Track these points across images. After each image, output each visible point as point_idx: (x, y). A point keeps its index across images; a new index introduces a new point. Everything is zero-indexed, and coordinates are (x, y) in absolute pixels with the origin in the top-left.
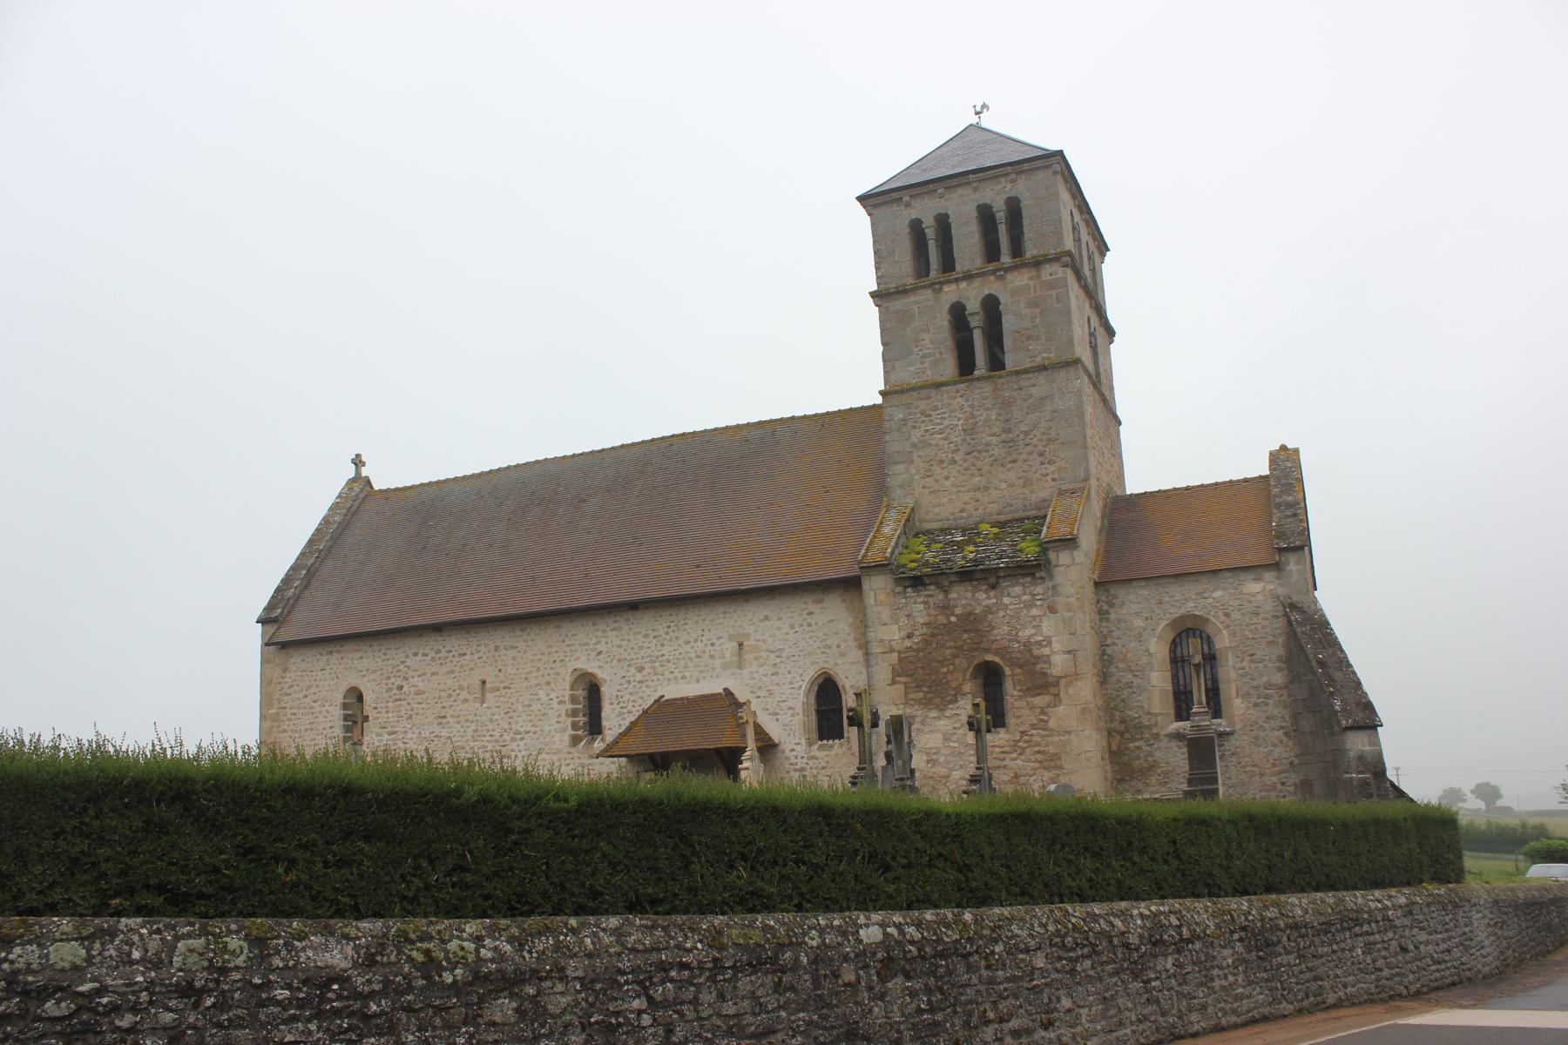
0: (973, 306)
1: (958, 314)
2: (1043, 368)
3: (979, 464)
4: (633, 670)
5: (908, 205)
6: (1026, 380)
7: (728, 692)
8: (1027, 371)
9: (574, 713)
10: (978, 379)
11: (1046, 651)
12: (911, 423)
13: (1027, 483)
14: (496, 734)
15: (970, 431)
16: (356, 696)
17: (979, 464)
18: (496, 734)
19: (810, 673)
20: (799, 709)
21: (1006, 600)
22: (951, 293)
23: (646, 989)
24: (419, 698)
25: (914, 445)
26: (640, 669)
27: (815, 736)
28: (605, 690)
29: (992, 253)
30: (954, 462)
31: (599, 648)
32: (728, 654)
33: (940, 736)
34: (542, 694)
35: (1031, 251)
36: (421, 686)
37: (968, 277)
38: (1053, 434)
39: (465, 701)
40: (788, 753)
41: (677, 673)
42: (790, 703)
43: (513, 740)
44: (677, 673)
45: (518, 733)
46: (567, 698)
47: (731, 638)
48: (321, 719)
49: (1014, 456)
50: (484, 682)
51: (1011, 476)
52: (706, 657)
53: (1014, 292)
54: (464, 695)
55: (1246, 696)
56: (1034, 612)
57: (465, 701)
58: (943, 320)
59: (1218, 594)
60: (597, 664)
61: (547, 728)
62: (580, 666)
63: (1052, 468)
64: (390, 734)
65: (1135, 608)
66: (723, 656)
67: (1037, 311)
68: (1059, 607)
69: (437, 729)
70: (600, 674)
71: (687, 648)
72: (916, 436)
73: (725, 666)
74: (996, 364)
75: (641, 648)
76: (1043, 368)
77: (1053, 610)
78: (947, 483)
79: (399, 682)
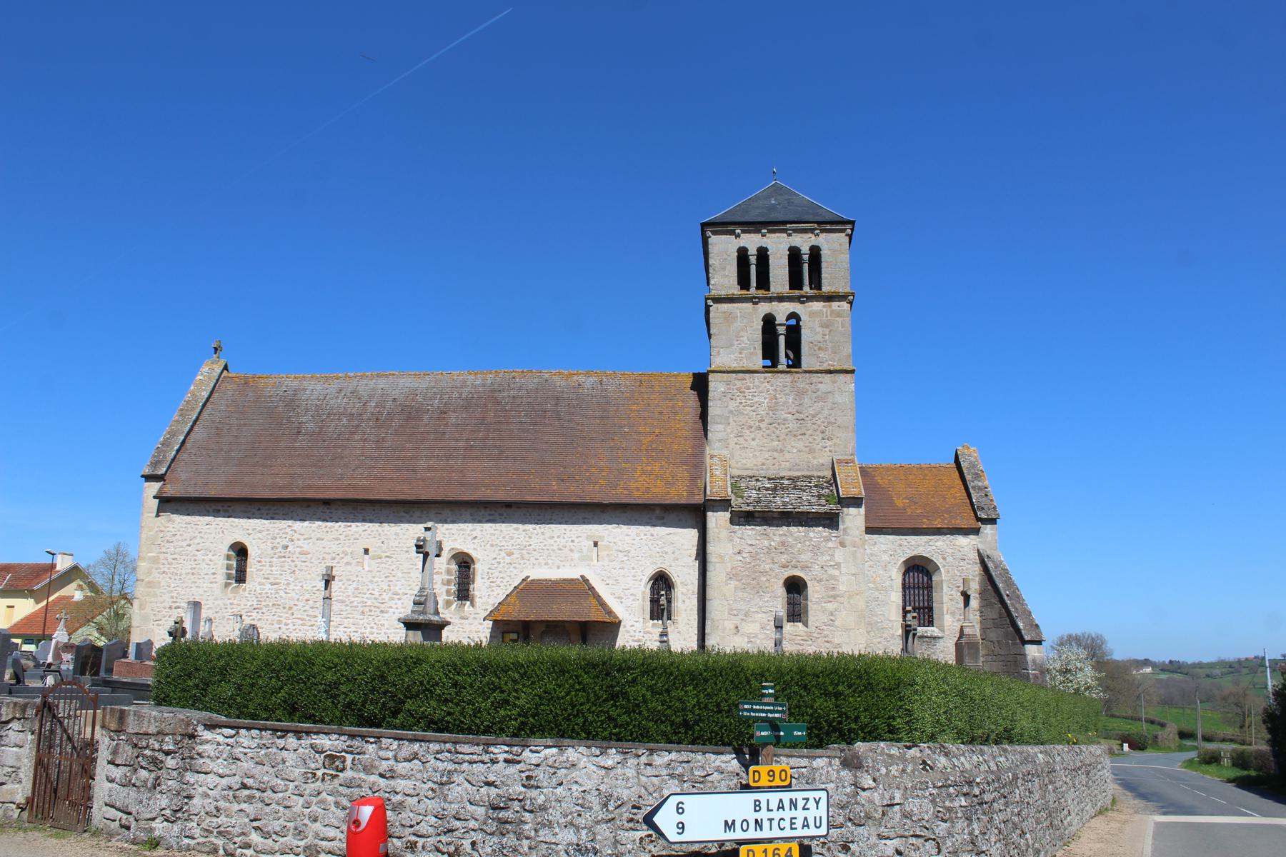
0: (781, 319)
1: (769, 321)
2: (830, 372)
3: (777, 432)
4: (503, 554)
5: (738, 236)
6: (815, 378)
7: (585, 580)
8: (817, 372)
9: (448, 582)
10: (782, 372)
11: (836, 572)
12: (729, 396)
13: (811, 451)
14: (376, 593)
15: (773, 408)
16: (240, 551)
17: (777, 432)
18: (376, 593)
19: (651, 571)
20: (639, 596)
21: (812, 534)
22: (765, 308)
23: (520, 801)
24: (303, 558)
25: (731, 412)
26: (510, 554)
27: (648, 616)
28: (479, 569)
29: (795, 282)
30: (760, 428)
31: (475, 534)
32: (585, 550)
33: (758, 625)
35: (826, 288)
36: (306, 548)
37: (781, 298)
38: (832, 420)
39: (348, 563)
40: (628, 628)
41: (541, 560)
42: (632, 591)
43: (392, 599)
44: (541, 560)
46: (443, 570)
47: (588, 538)
48: (203, 565)
49: (803, 431)
51: (800, 444)
52: (566, 550)
53: (812, 314)
54: (348, 559)
55: (953, 613)
56: (830, 544)
57: (348, 563)
58: (759, 325)
59: (938, 544)
63: (829, 443)
64: (272, 584)
65: (883, 547)
66: (580, 551)
67: (827, 331)
68: (847, 543)
70: (474, 554)
71: (551, 542)
72: (732, 405)
73: (582, 559)
74: (796, 363)
75: (512, 538)
76: (830, 372)
77: (842, 544)
78: (754, 443)
79: (285, 542)
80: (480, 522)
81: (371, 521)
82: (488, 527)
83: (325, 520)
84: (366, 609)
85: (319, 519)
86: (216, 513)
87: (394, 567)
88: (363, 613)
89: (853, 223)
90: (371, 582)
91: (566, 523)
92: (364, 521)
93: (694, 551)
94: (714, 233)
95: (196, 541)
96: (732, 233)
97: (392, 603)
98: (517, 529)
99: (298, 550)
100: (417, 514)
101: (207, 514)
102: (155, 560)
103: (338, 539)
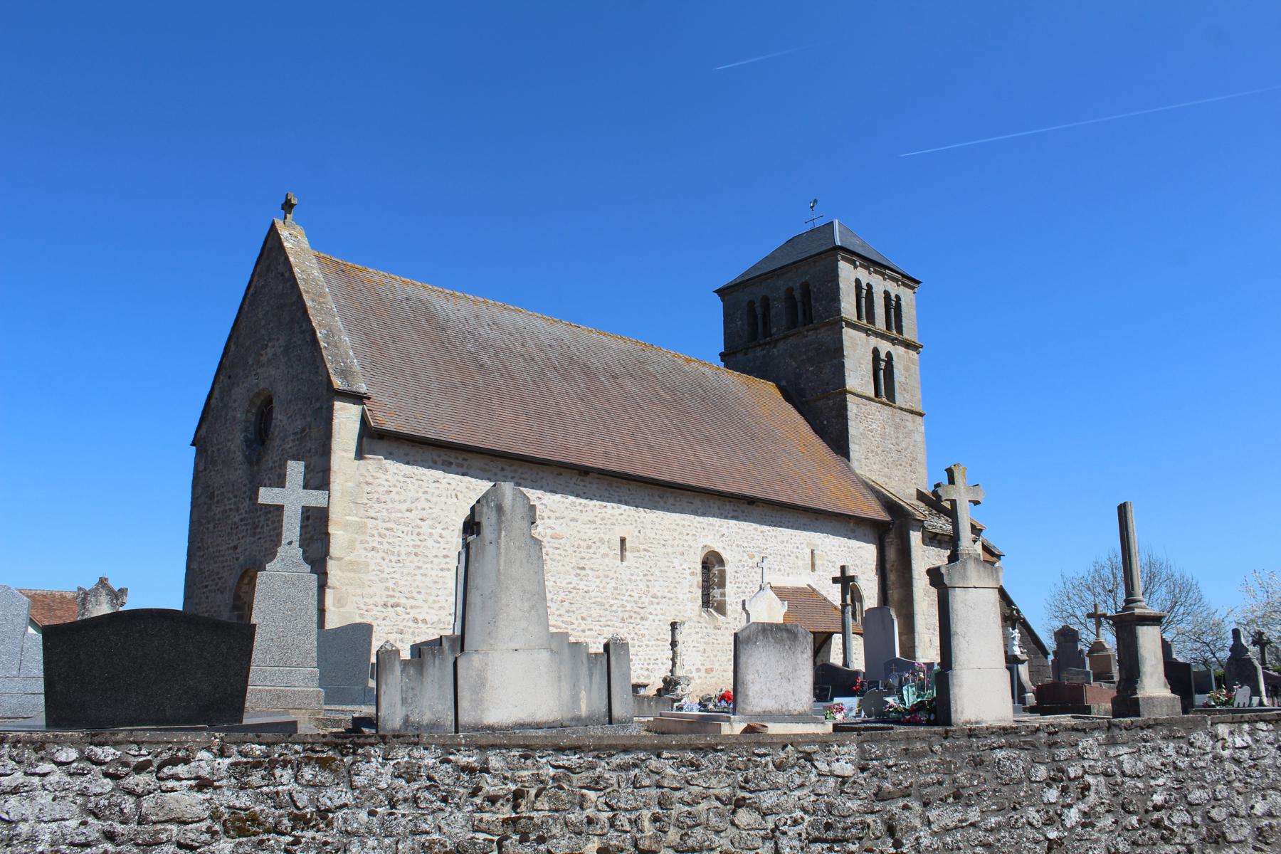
4: (746, 557)
34: (676, 562)
36: (558, 530)
45: (655, 597)
48: (430, 543)
50: (623, 541)
57: (605, 555)
60: (722, 545)
61: (681, 596)
62: (708, 543)
69: (575, 580)
75: (753, 539)
80: (726, 518)
81: (627, 504)
82: (733, 522)
83: (577, 496)
84: (626, 615)
85: (572, 493)
86: (447, 467)
87: (651, 563)
88: (623, 620)
89: (918, 282)
90: (630, 580)
91: (792, 527)
92: (620, 502)
93: (873, 566)
94: (844, 259)
95: (420, 505)
96: (853, 263)
97: (651, 609)
98: (756, 529)
99: (549, 531)
100: (671, 501)
101: (433, 465)
102: (360, 528)
103: (594, 522)
